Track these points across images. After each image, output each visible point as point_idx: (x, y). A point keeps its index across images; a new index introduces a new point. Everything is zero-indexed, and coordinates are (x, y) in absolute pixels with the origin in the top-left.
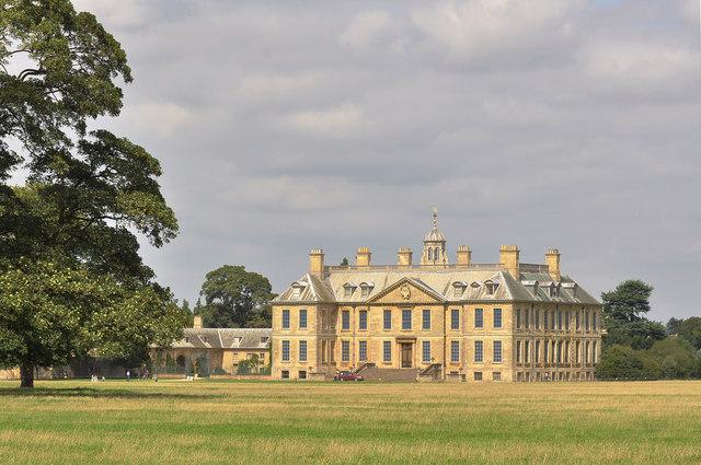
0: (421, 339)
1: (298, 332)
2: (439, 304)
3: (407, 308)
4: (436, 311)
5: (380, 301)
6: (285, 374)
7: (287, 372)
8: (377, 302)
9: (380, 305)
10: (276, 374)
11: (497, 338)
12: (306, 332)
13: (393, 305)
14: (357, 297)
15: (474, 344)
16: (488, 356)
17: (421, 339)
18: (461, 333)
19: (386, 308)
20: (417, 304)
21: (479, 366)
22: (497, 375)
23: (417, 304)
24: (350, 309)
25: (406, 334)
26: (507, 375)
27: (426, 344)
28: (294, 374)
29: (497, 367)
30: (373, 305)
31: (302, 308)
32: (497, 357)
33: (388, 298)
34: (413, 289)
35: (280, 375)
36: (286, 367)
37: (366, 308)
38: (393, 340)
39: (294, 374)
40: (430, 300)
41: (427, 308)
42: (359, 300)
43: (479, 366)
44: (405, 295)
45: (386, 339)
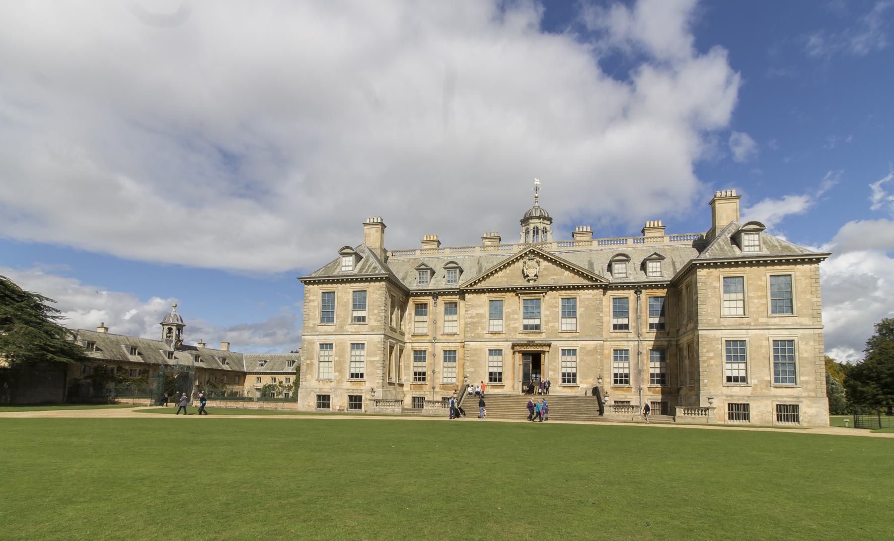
1: (350, 329)
2: (592, 288)
6: (324, 400)
7: (328, 397)
8: (479, 286)
9: (483, 291)
10: (307, 403)
12: (364, 329)
14: (439, 282)
18: (632, 336)
23: (552, 289)
24: (429, 300)
25: (532, 337)
30: (471, 292)
31: (358, 286)
34: (544, 264)
35: (313, 402)
36: (326, 389)
37: (455, 298)
38: (506, 347)
39: (339, 402)
42: (443, 285)
44: (531, 273)
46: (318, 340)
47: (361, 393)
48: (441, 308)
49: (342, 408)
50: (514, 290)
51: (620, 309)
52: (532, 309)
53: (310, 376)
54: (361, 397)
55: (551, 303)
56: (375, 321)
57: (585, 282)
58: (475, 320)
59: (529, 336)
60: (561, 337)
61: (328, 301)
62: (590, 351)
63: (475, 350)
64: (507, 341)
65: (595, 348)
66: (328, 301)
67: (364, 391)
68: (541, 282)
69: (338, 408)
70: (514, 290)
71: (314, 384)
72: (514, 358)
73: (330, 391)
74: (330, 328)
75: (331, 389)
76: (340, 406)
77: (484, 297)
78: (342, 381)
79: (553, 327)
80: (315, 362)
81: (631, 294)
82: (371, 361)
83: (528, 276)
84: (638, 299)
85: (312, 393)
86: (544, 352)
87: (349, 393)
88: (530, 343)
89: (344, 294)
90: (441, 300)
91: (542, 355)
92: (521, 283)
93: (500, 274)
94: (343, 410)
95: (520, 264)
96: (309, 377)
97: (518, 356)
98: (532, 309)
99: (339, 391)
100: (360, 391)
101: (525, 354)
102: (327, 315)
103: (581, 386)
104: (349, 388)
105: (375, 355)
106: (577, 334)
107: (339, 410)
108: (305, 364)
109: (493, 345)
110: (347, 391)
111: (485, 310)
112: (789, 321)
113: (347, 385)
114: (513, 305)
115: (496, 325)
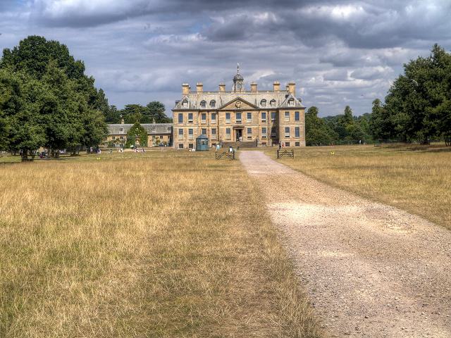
3: (238, 112)
5: (224, 109)
9: (224, 111)
11: (297, 126)
12: (193, 125)
15: (284, 129)
16: (292, 135)
19: (227, 112)
20: (244, 110)
22: (297, 144)
23: (244, 110)
26: (303, 143)
29: (297, 140)
32: (297, 133)
33: (229, 107)
37: (215, 112)
39: (186, 146)
40: (251, 108)
46: (178, 128)
48: (210, 115)
50: (233, 111)
51: (264, 116)
52: (239, 116)
55: (244, 115)
61: (181, 116)
66: (181, 116)
68: (241, 109)
70: (233, 111)
71: (178, 141)
74: (182, 125)
77: (224, 113)
88: (238, 127)
89: (186, 115)
90: (210, 113)
92: (235, 108)
98: (239, 116)
102: (181, 120)
109: (227, 127)
111: (225, 116)
112: (298, 123)
114: (233, 115)
115: (228, 121)
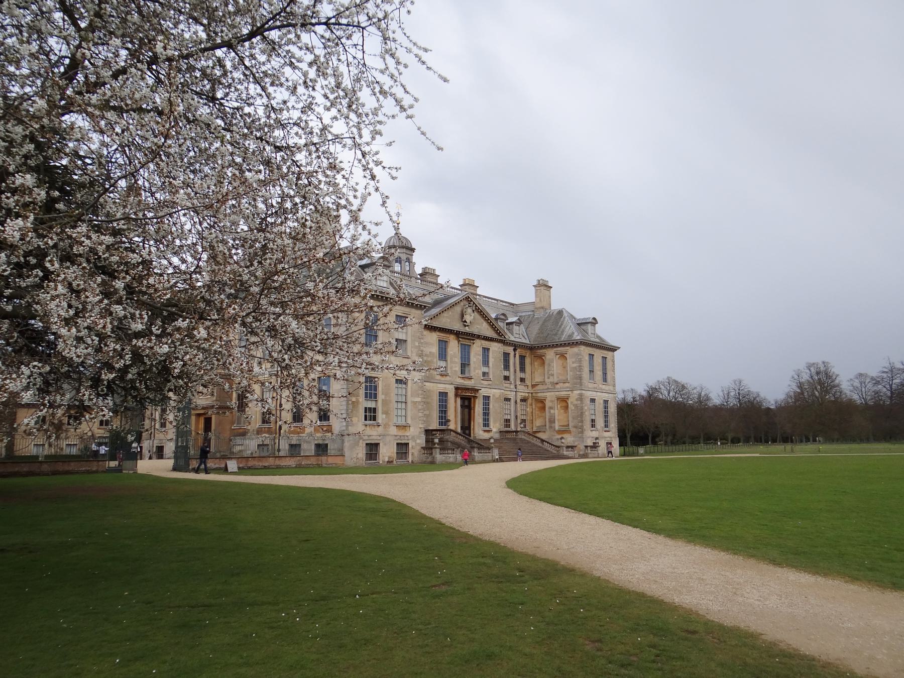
0: (484, 392)
4: (496, 349)
7: (377, 445)
13: (450, 332)
17: (484, 392)
18: (512, 386)
20: (479, 337)
21: (595, 434)
23: (479, 337)
26: (616, 443)
27: (487, 398)
28: (387, 452)
36: (373, 434)
39: (387, 452)
40: (490, 333)
41: (486, 344)
43: (595, 434)
44: (468, 318)
45: (442, 387)
47: (408, 440)
49: (391, 460)
50: (458, 334)
53: (357, 419)
54: (407, 444)
56: (417, 356)
57: (495, 336)
58: (429, 359)
59: (465, 380)
60: (482, 384)
62: (497, 398)
63: (429, 391)
64: (452, 384)
65: (500, 396)
67: (410, 437)
69: (387, 460)
70: (458, 334)
72: (456, 402)
73: (379, 438)
75: (380, 436)
76: (389, 457)
78: (389, 425)
79: (478, 374)
80: (361, 400)
81: (510, 350)
82: (414, 402)
83: (465, 322)
84: (515, 354)
85: (361, 441)
86: (475, 397)
87: (397, 440)
91: (472, 400)
92: (457, 326)
93: (445, 314)
94: (392, 462)
95: (458, 309)
96: (355, 419)
97: (459, 400)
99: (388, 438)
100: (406, 438)
101: (463, 399)
103: (494, 430)
104: (396, 434)
105: (418, 396)
106: (491, 382)
107: (388, 462)
108: (350, 402)
110: (395, 438)
113: (393, 431)
